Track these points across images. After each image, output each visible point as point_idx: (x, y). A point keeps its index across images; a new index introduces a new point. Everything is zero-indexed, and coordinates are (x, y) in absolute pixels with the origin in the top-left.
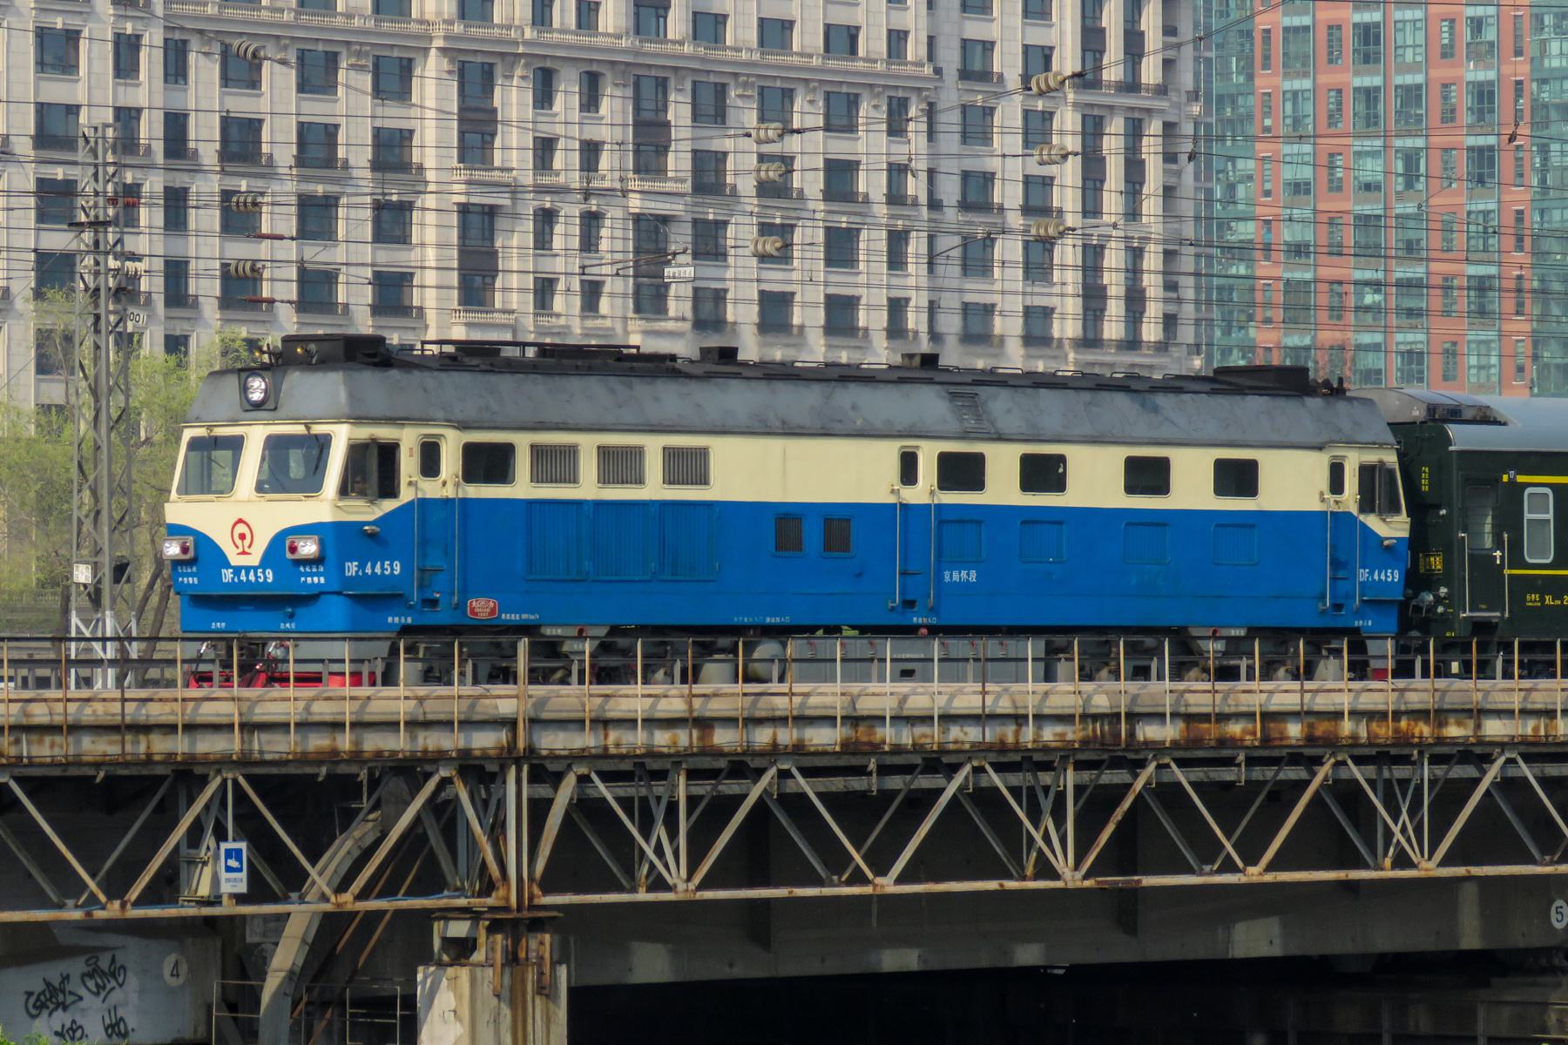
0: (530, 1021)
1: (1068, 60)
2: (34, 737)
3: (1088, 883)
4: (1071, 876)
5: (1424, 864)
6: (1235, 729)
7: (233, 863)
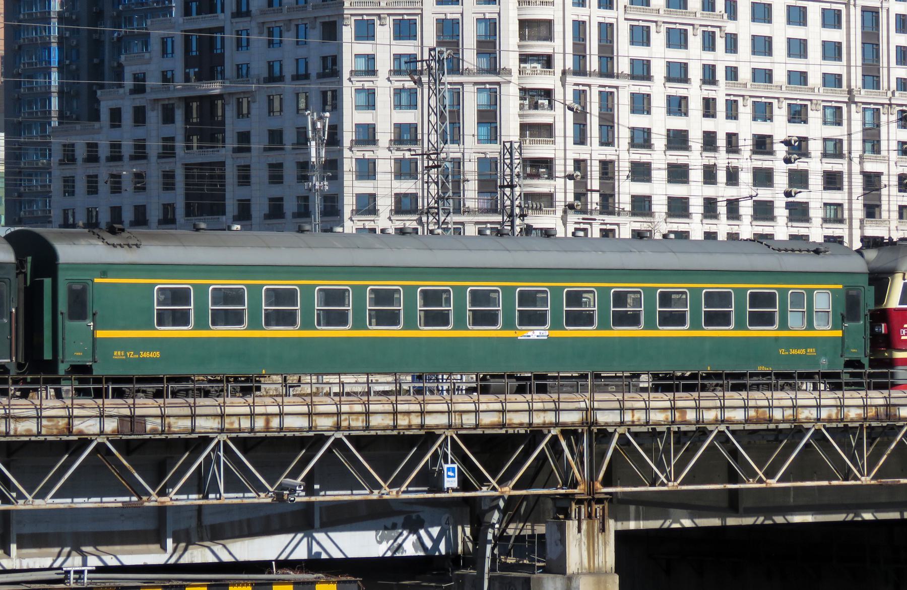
0: (596, 545)
2: (354, 417)
3: (873, 482)
4: (866, 480)
7: (451, 474)
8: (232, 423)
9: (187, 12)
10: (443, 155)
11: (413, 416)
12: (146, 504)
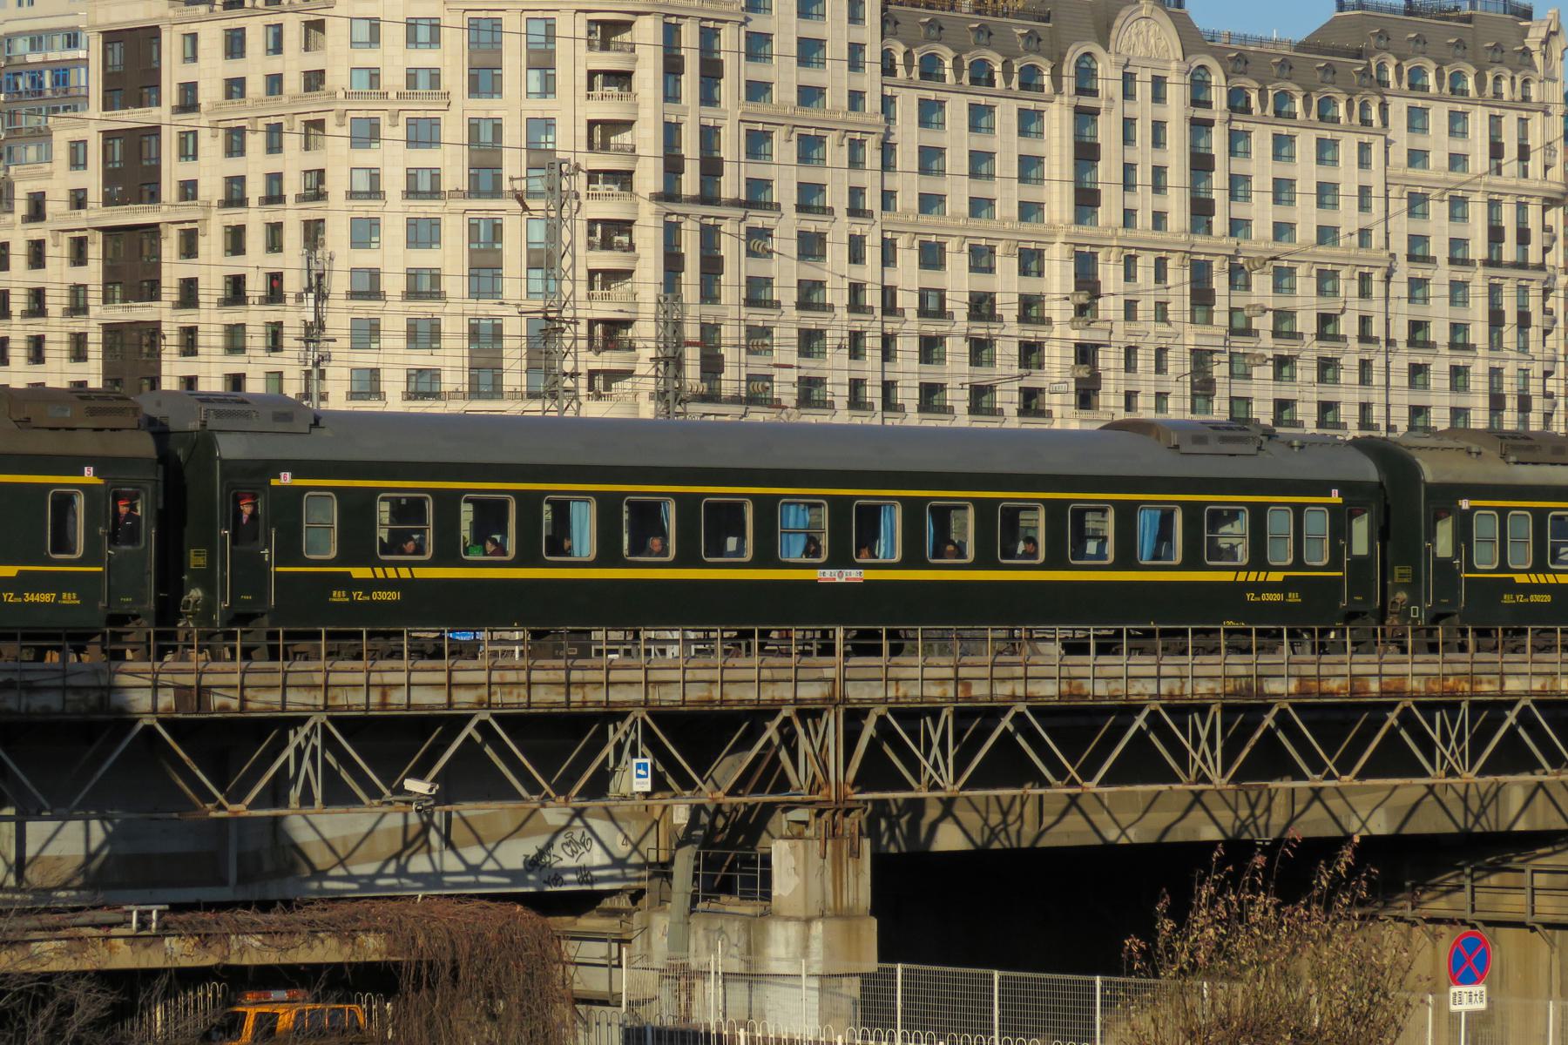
1: (1478, 249)
2: (506, 690)
5: (1466, 775)
6: (1333, 685)
7: (641, 772)
8: (334, 698)
9: (107, 106)
10: (567, 314)
11: (588, 689)
12: (213, 814)
